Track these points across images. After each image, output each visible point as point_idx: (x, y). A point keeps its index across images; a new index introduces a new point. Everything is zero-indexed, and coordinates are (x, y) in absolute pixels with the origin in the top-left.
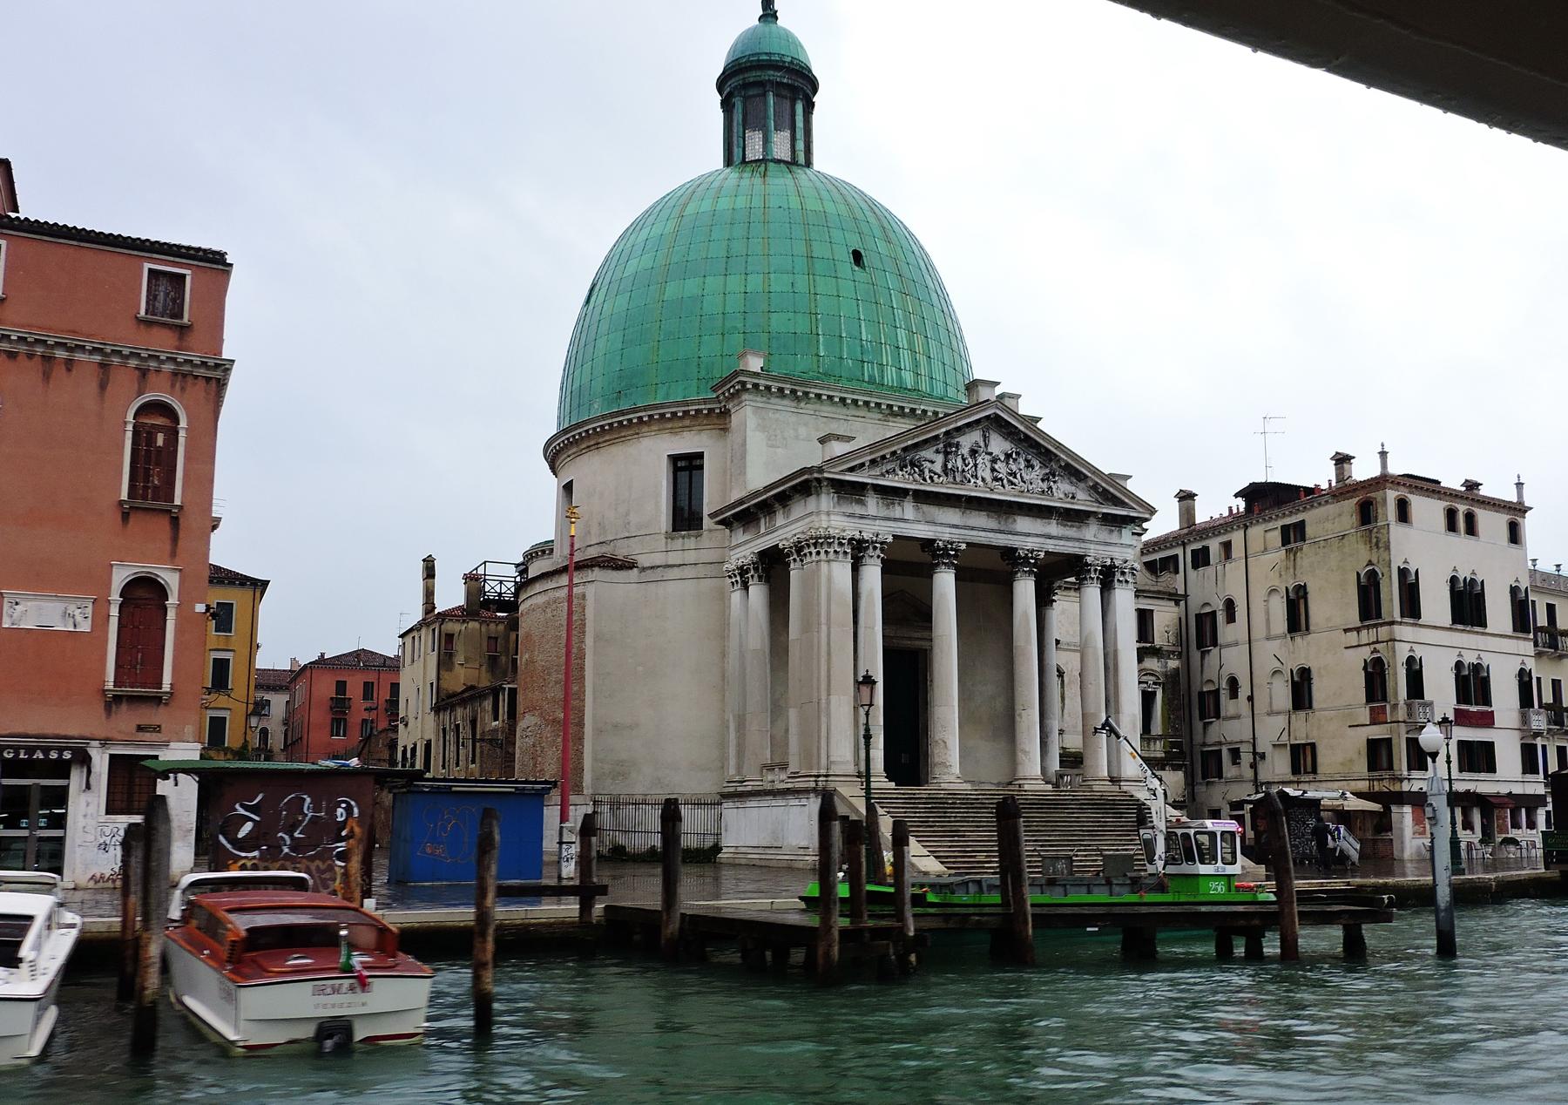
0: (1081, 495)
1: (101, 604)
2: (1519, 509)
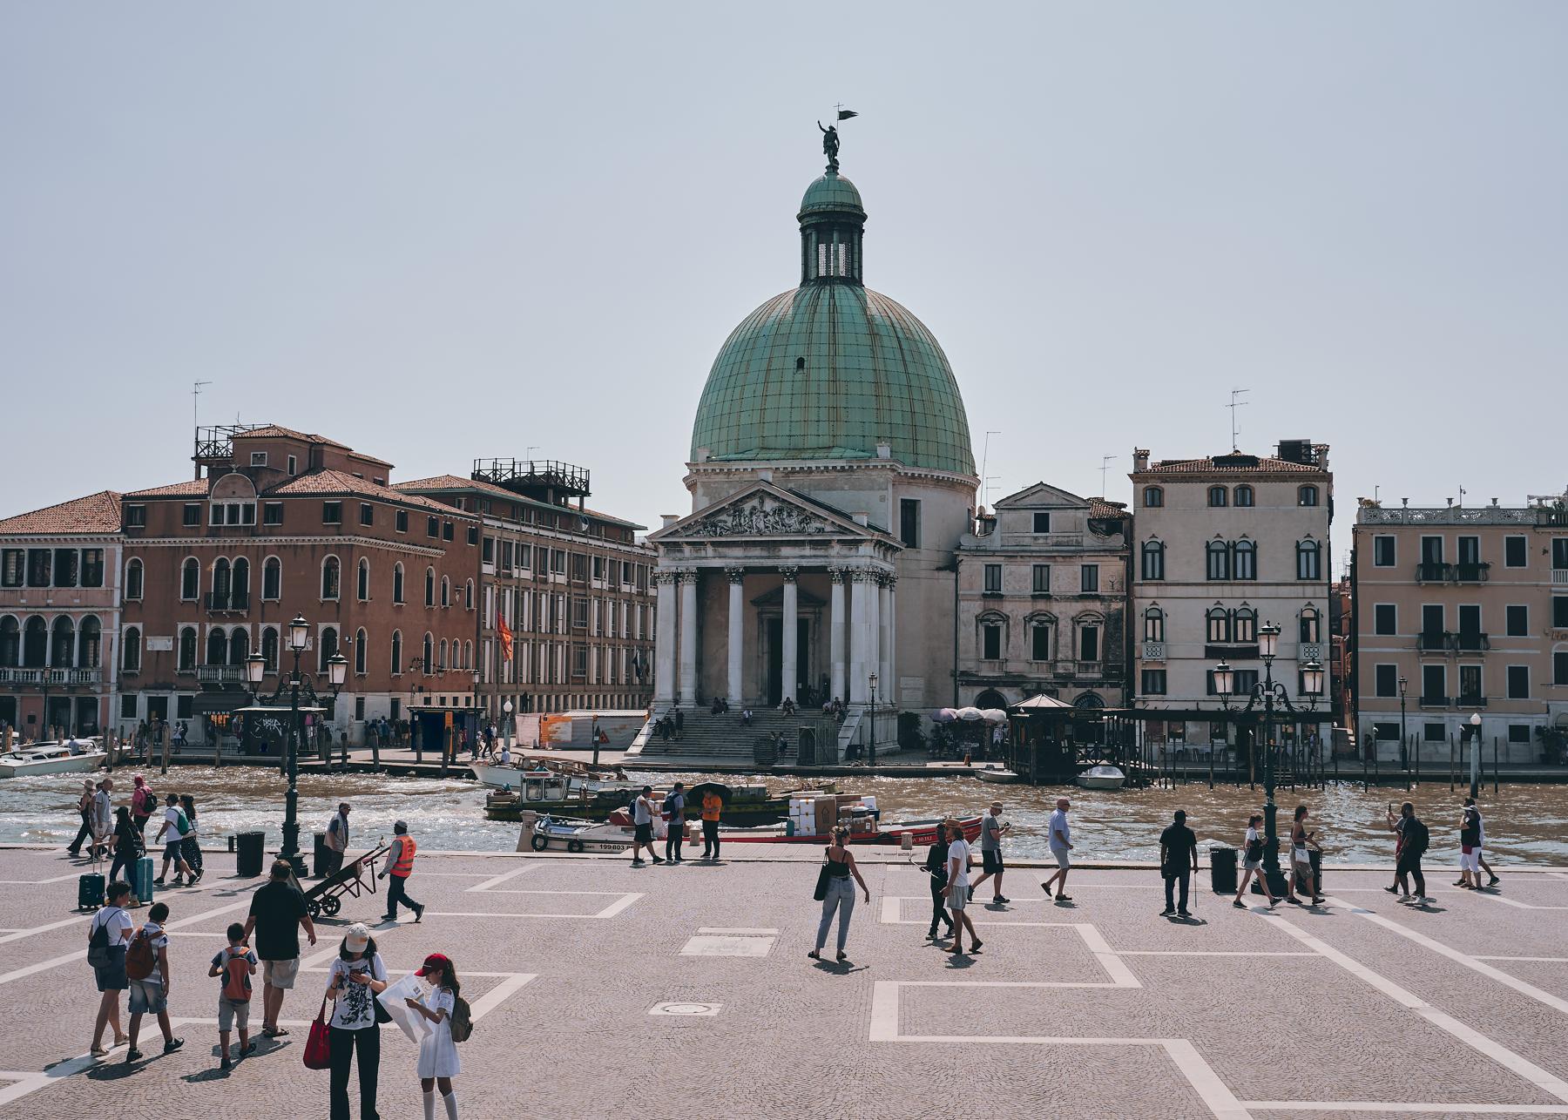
1: (315, 640)
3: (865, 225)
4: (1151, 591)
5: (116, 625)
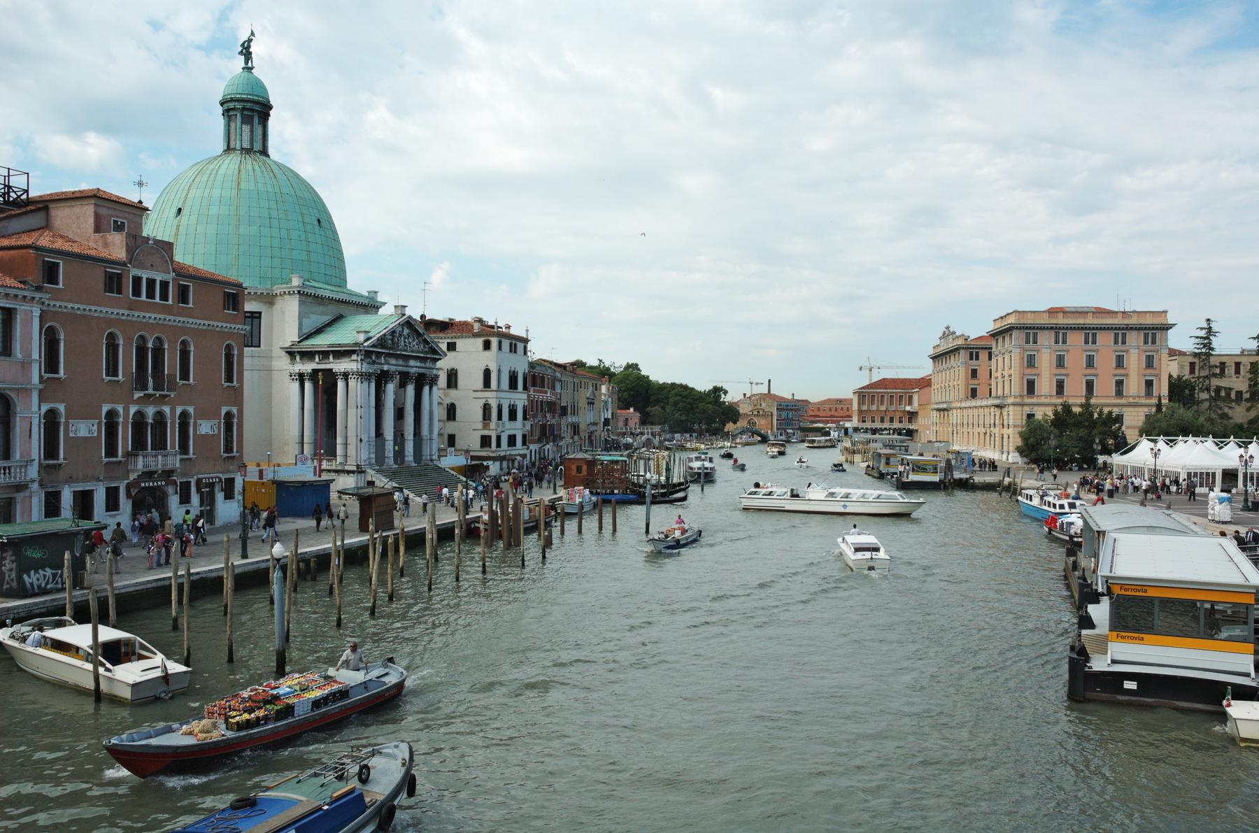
2: (525, 341)
5: (35, 408)
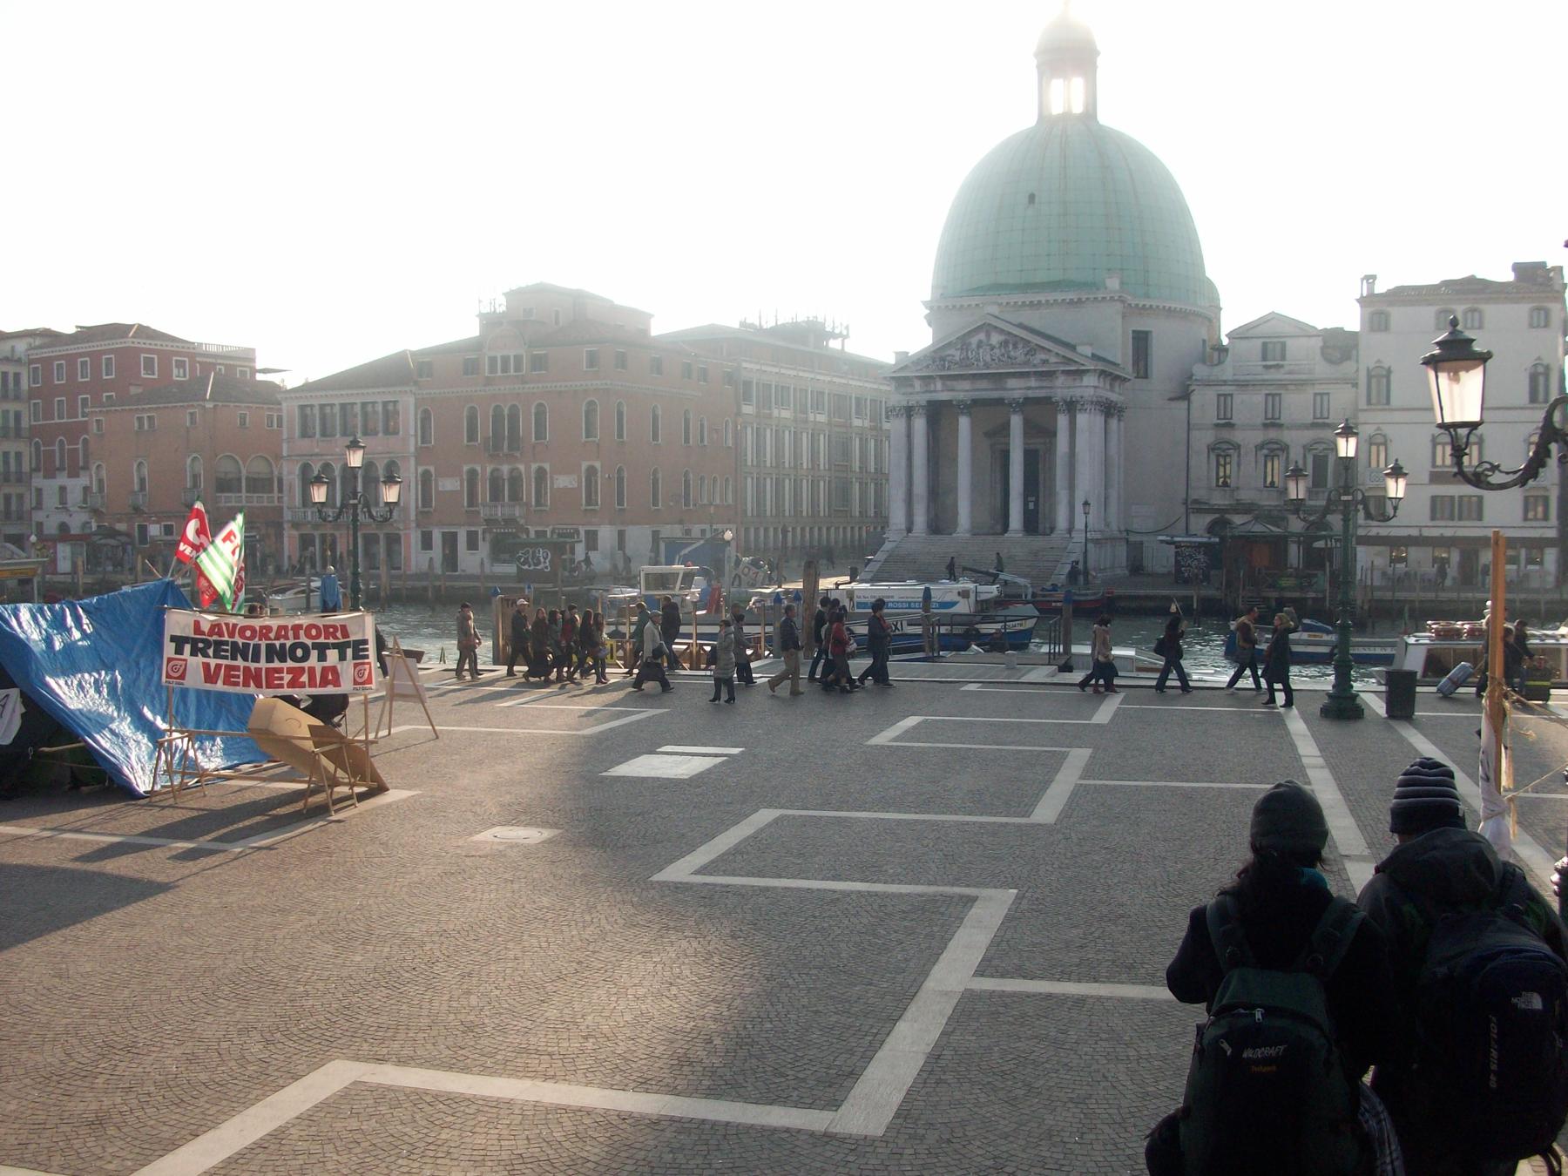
0: (1053, 359)
3: (1100, 61)
4: (1380, 417)
5: (412, 469)
